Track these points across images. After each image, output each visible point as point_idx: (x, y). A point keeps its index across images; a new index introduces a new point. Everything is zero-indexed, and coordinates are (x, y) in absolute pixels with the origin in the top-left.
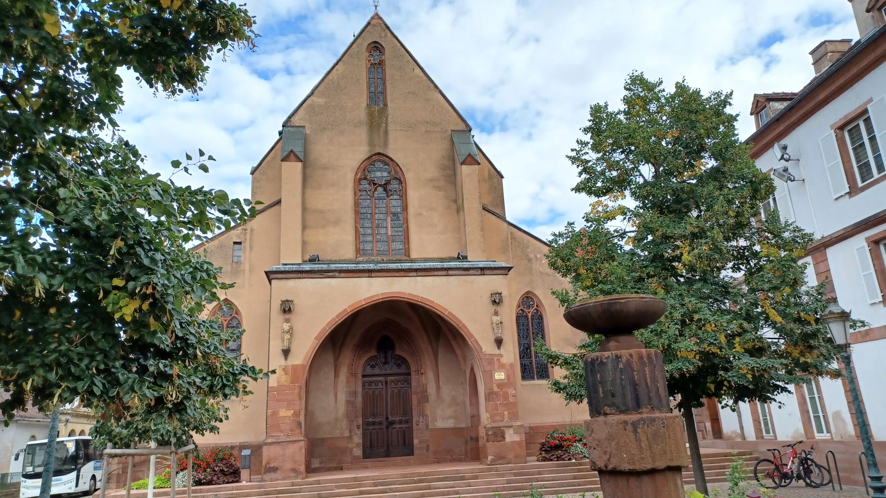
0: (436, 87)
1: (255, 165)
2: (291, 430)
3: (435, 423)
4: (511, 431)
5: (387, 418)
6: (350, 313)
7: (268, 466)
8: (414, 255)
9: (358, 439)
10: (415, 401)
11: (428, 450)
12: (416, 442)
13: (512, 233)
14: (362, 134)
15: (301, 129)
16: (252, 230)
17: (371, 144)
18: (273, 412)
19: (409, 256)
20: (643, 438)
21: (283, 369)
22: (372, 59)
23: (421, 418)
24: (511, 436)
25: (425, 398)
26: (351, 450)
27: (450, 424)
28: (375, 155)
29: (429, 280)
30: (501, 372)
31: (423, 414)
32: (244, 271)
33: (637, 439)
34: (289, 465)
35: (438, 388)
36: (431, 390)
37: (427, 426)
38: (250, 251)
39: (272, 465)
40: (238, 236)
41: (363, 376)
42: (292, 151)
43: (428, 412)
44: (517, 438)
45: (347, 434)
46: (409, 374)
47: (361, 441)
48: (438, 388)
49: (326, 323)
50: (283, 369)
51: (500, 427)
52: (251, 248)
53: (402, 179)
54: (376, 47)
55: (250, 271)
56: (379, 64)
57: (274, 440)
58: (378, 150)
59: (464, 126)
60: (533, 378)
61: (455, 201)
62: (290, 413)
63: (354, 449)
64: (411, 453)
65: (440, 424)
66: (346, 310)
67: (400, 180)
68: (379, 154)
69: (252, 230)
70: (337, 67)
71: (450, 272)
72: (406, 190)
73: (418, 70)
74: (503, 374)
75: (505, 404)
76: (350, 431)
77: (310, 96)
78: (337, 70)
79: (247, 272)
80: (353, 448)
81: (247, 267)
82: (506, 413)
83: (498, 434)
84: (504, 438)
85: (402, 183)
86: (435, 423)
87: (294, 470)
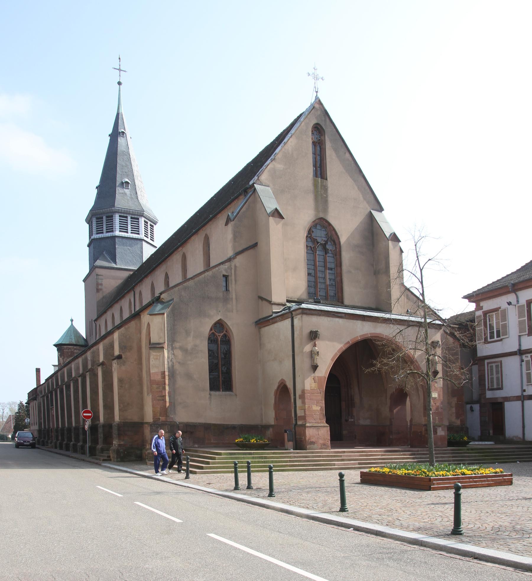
0: (361, 171)
2: (320, 419)
7: (309, 441)
8: (346, 302)
14: (310, 201)
15: (267, 188)
16: (235, 266)
17: (317, 209)
18: (309, 407)
22: (313, 137)
28: (318, 219)
30: (436, 393)
32: (232, 299)
34: (321, 442)
40: (226, 270)
52: (236, 281)
53: (337, 241)
54: (318, 129)
55: (236, 299)
58: (321, 215)
59: (379, 208)
61: (373, 265)
62: (319, 408)
66: (348, 342)
67: (334, 242)
68: (321, 219)
69: (235, 266)
73: (347, 155)
74: (436, 394)
81: (234, 297)
87: (324, 445)
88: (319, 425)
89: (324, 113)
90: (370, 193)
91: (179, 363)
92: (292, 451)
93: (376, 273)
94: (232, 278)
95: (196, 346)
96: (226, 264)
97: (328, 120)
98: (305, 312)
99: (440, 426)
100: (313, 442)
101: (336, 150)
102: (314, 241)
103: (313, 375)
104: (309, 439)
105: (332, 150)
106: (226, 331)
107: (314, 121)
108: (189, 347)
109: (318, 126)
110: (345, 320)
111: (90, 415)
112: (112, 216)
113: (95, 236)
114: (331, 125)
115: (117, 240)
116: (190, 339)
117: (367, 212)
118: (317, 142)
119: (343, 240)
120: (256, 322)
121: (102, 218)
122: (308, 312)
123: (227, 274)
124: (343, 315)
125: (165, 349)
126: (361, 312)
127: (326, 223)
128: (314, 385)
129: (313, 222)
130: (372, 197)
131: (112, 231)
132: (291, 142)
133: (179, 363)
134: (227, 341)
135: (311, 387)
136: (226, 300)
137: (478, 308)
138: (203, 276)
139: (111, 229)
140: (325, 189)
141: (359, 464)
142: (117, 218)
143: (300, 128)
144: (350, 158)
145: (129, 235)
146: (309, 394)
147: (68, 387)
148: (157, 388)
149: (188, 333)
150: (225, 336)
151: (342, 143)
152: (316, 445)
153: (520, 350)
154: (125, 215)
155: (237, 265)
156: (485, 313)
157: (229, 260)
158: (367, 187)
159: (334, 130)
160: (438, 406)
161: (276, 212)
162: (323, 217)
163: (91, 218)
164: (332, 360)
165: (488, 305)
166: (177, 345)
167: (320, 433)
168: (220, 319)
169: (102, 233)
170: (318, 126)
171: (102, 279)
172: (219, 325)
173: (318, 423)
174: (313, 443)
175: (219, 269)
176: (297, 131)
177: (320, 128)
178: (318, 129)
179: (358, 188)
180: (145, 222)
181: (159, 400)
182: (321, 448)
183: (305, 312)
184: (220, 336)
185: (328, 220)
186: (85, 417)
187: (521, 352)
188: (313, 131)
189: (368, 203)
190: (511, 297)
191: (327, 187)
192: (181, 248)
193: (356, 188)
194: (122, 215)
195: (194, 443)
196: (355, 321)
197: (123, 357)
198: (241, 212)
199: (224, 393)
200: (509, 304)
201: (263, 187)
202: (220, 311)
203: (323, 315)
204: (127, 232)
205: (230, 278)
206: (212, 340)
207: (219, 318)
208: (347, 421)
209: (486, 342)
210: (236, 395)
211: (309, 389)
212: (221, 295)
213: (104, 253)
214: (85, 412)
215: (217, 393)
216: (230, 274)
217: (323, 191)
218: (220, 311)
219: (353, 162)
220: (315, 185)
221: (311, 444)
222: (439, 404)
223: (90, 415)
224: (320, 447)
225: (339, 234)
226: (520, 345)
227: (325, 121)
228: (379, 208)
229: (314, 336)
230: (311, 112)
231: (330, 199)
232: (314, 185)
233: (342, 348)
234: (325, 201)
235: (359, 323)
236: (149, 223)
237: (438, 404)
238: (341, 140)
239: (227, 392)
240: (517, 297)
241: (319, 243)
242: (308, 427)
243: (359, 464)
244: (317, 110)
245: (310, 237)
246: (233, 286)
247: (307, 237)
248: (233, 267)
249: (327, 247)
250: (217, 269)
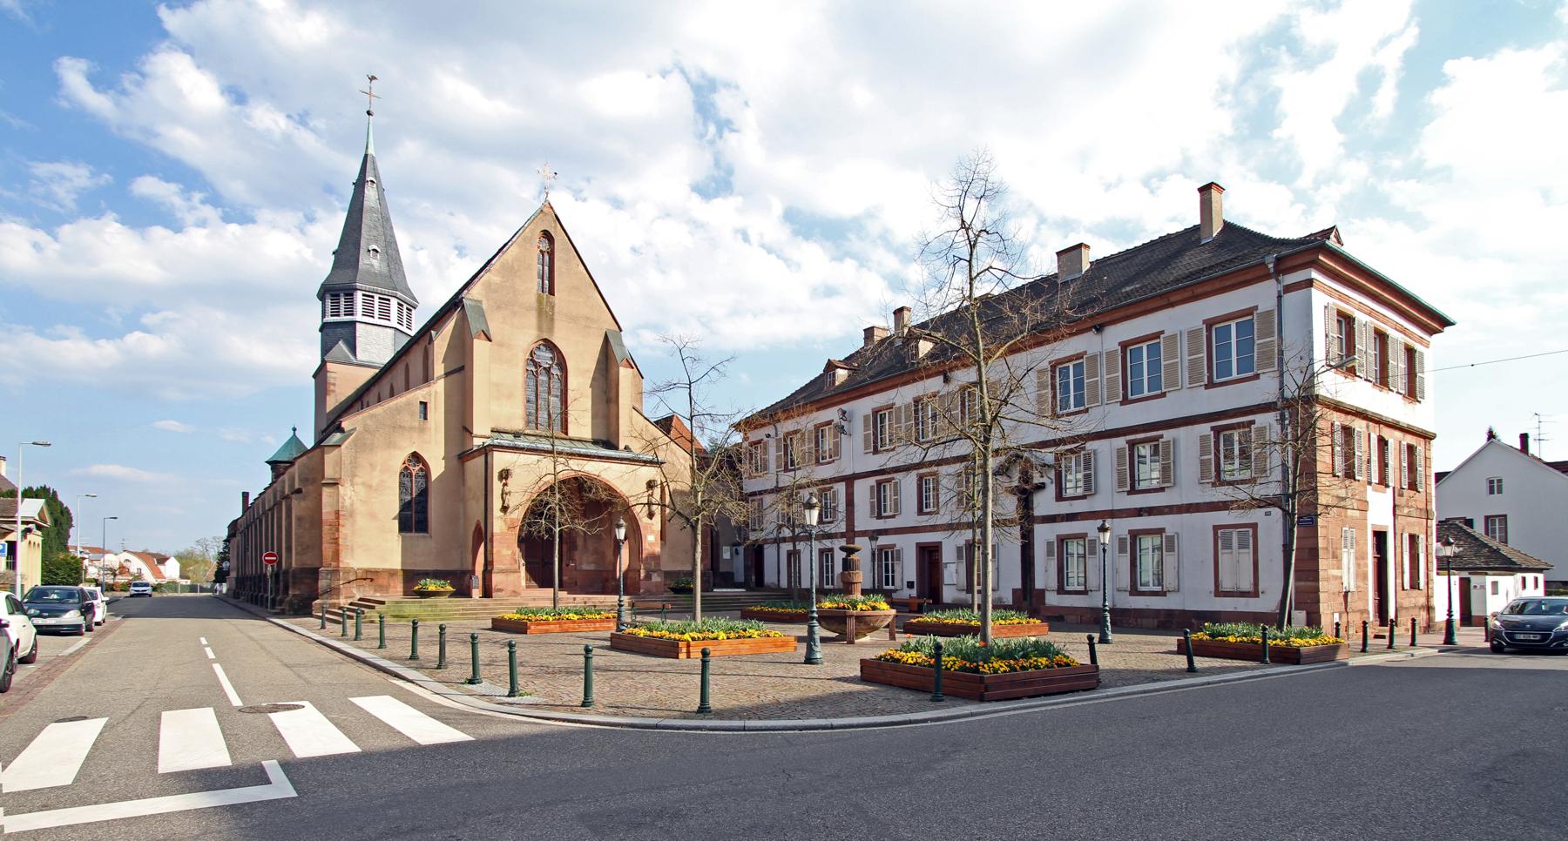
4: (656, 575)
11: (576, 585)
13: (646, 426)
16: (436, 393)
19: (566, 434)
27: (592, 567)
32: (430, 429)
38: (435, 412)
39: (499, 587)
44: (659, 579)
52: (435, 408)
55: (436, 429)
61: (605, 393)
62: (510, 552)
65: (585, 567)
69: (436, 393)
79: (433, 430)
91: (361, 501)
93: (608, 401)
99: (654, 572)
102: (536, 365)
108: (374, 483)
111: (274, 558)
112: (352, 295)
113: (329, 319)
115: (358, 324)
116: (376, 473)
120: (459, 455)
121: (339, 295)
131: (352, 315)
133: (361, 501)
136: (422, 430)
137: (745, 439)
139: (350, 312)
142: (359, 296)
145: (376, 321)
147: (261, 521)
148: (330, 530)
153: (777, 487)
154: (371, 294)
156: (751, 444)
163: (324, 294)
165: (755, 435)
166: (357, 480)
169: (338, 315)
171: (335, 378)
180: (399, 304)
181: (332, 543)
184: (415, 469)
186: (267, 561)
187: (777, 490)
190: (770, 430)
192: (404, 358)
194: (367, 293)
195: (376, 591)
197: (303, 490)
200: (768, 436)
204: (373, 317)
205: (428, 405)
208: (567, 565)
209: (750, 477)
210: (431, 537)
213: (340, 342)
214: (267, 556)
223: (274, 558)
226: (777, 482)
236: (405, 306)
239: (421, 534)
240: (776, 429)
245: (532, 360)
249: (552, 371)
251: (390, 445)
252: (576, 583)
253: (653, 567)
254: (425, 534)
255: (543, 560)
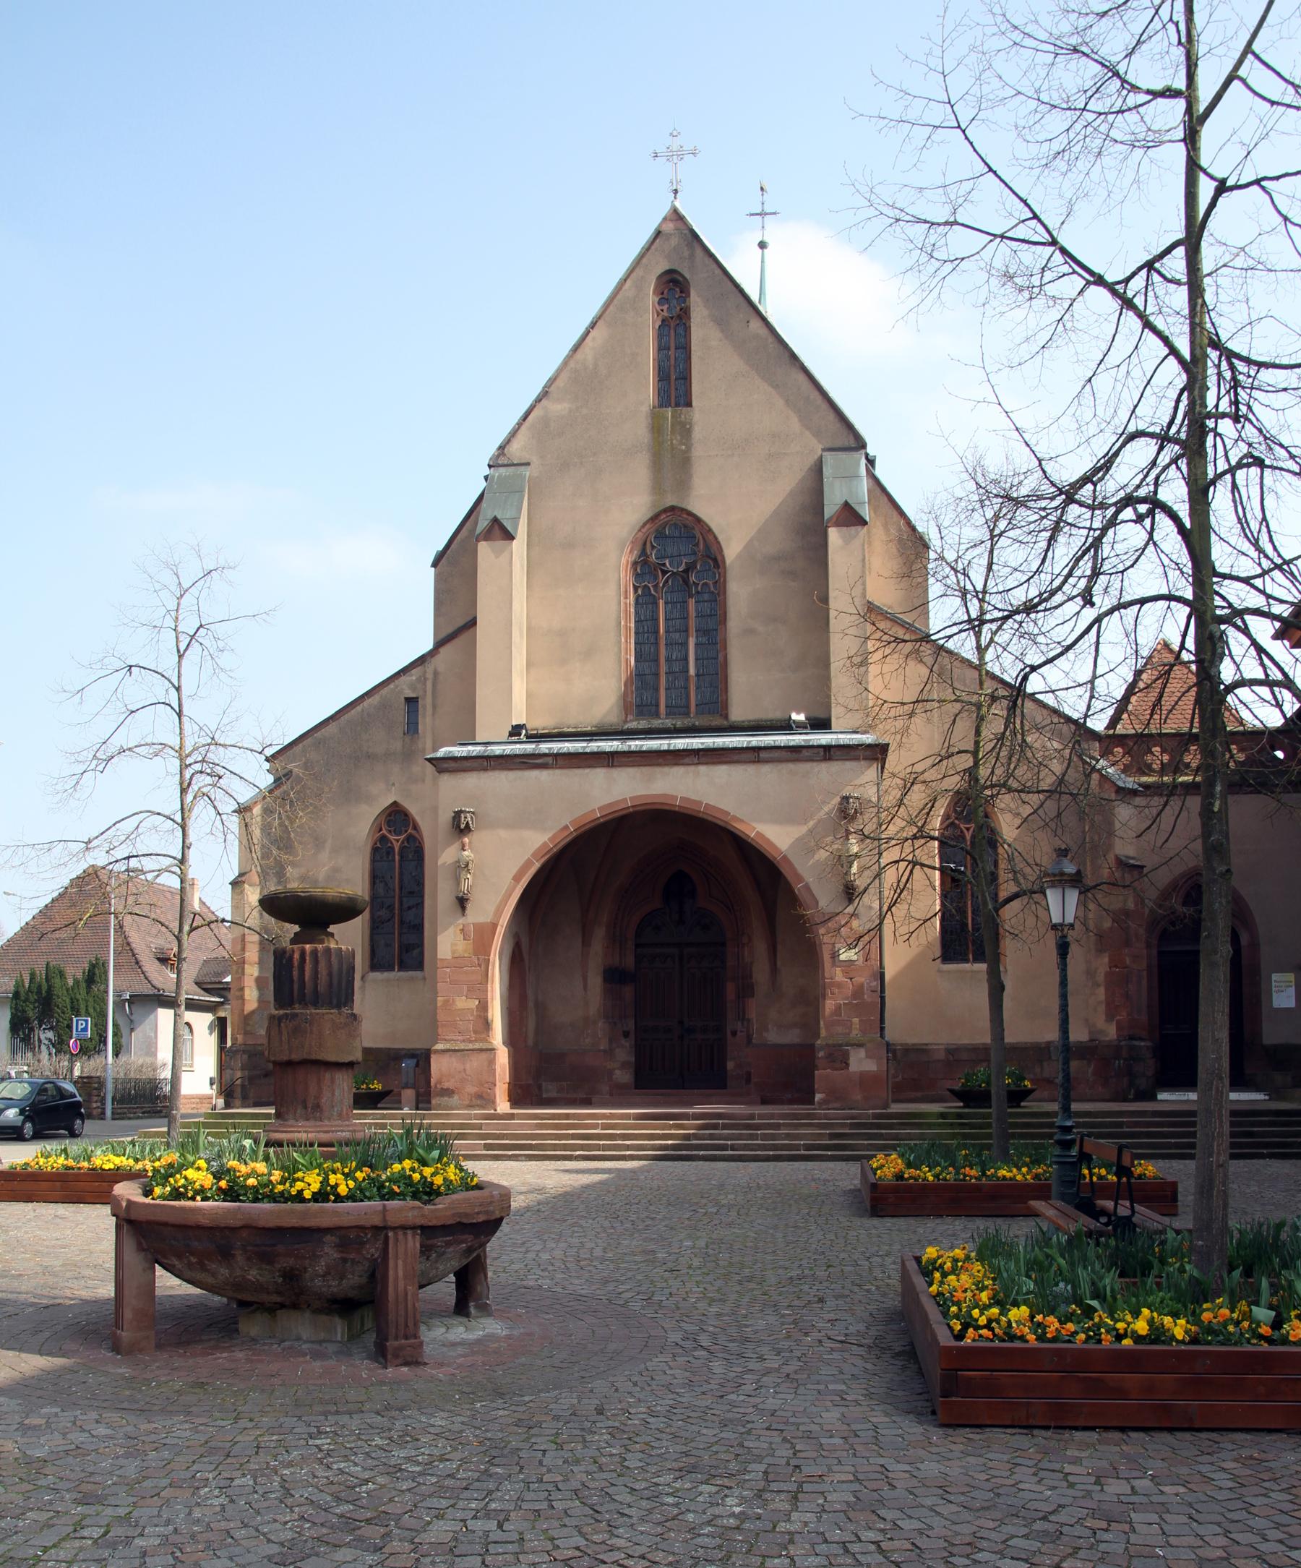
0: (794, 357)
1: (441, 548)
2: (475, 1032)
3: (765, 1034)
4: (862, 1053)
5: (681, 1022)
6: (575, 834)
8: (738, 713)
9: (624, 1053)
10: (731, 990)
11: (748, 1080)
12: (730, 1065)
14: (640, 471)
15: (522, 468)
16: (436, 674)
17: (657, 487)
18: (446, 1002)
19: (726, 717)
20: (285, 1033)
21: (462, 930)
22: (665, 307)
23: (739, 1023)
24: (861, 1062)
25: (746, 990)
26: (611, 1073)
28: (665, 511)
29: (721, 772)
31: (742, 1016)
33: (280, 1032)
34: (471, 1089)
35: (774, 970)
36: (760, 974)
37: (749, 1038)
38: (434, 714)
39: (446, 1085)
41: (637, 946)
42: (496, 520)
43: (752, 1014)
44: (870, 1066)
45: (603, 1045)
46: (723, 944)
47: (633, 1059)
48: (774, 970)
49: (532, 851)
50: (462, 930)
51: (841, 1045)
52: (434, 707)
53: (719, 558)
56: (679, 317)
57: (448, 1046)
58: (670, 501)
60: (967, 961)
63: (618, 1072)
64: (725, 1087)
65: (774, 1037)
66: (566, 827)
67: (715, 560)
68: (672, 509)
69: (436, 674)
70: (593, 333)
71: (763, 755)
72: (725, 581)
73: (755, 325)
75: (856, 1004)
76: (611, 1041)
77: (540, 400)
78: (594, 339)
80: (614, 1069)
82: (856, 1020)
83: (839, 1057)
84: (847, 1065)
85: (718, 567)
86: (765, 1034)
87: (479, 1096)
88: (470, 1046)
89: (689, 236)
90: (825, 406)
92: (406, 1111)
94: (426, 703)
95: (336, 870)
96: (414, 671)
97: (699, 252)
98: (446, 765)
99: (860, 1045)
100: (448, 1089)
101: (721, 322)
103: (461, 921)
104: (439, 1082)
105: (712, 323)
106: (381, 830)
107: (662, 266)
109: (675, 276)
110: (558, 772)
114: (708, 261)
116: (324, 856)
117: (811, 460)
118: (672, 318)
119: (732, 551)
122: (453, 765)
123: (414, 695)
124: (549, 760)
125: (250, 885)
126: (615, 743)
127: (690, 518)
128: (463, 947)
129: (654, 518)
130: (831, 416)
132: (594, 339)
134: (414, 852)
135: (453, 952)
138: (359, 708)
140: (685, 430)
141: (487, 1147)
143: (619, 297)
144: (764, 332)
146: (448, 970)
149: (319, 842)
150: (410, 838)
151: (741, 299)
152: (456, 1097)
155: (441, 669)
157: (422, 660)
158: (815, 394)
159: (718, 271)
160: (862, 985)
161: (496, 527)
162: (674, 503)
164: (517, 878)
167: (468, 1066)
168: (395, 803)
170: (675, 276)
172: (396, 817)
173: (470, 1041)
174: (448, 1092)
175: (397, 687)
176: (611, 308)
177: (680, 279)
178: (675, 282)
179: (787, 401)
182: (470, 1106)
183: (446, 765)
184: (396, 841)
185: (690, 508)
188: (666, 292)
189: (817, 434)
191: (690, 424)
193: (780, 403)
196: (587, 771)
198: (455, 542)
199: (401, 973)
201: (511, 470)
202: (393, 784)
203: (494, 769)
206: (380, 851)
207: (391, 801)
211: (449, 957)
212: (397, 745)
215: (386, 975)
216: (420, 694)
217: (679, 438)
218: (393, 784)
219: (771, 339)
220: (656, 428)
221: (442, 1095)
222: (863, 979)
224: (467, 1102)
225: (720, 538)
227: (692, 256)
228: (853, 443)
229: (460, 828)
230: (653, 247)
231: (698, 452)
232: (653, 427)
233: (545, 844)
234: (684, 463)
235: (598, 776)
237: (859, 980)
238: (737, 292)
241: (667, 572)
242: (437, 1051)
243: (487, 1147)
244: (669, 236)
246: (428, 720)
247: (635, 564)
248: (430, 676)
250: (392, 686)
251: (350, 795)
252: (749, 1074)
253: (855, 1033)
254: (418, 974)
255: (681, 1022)
